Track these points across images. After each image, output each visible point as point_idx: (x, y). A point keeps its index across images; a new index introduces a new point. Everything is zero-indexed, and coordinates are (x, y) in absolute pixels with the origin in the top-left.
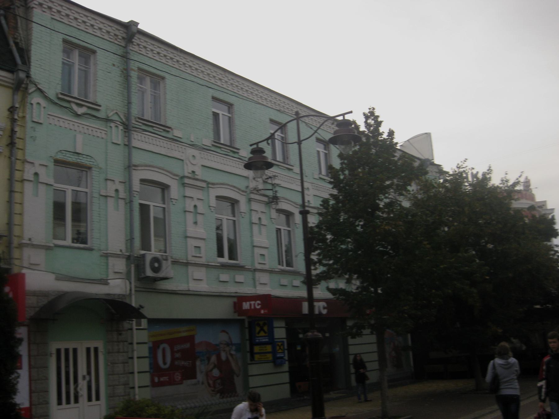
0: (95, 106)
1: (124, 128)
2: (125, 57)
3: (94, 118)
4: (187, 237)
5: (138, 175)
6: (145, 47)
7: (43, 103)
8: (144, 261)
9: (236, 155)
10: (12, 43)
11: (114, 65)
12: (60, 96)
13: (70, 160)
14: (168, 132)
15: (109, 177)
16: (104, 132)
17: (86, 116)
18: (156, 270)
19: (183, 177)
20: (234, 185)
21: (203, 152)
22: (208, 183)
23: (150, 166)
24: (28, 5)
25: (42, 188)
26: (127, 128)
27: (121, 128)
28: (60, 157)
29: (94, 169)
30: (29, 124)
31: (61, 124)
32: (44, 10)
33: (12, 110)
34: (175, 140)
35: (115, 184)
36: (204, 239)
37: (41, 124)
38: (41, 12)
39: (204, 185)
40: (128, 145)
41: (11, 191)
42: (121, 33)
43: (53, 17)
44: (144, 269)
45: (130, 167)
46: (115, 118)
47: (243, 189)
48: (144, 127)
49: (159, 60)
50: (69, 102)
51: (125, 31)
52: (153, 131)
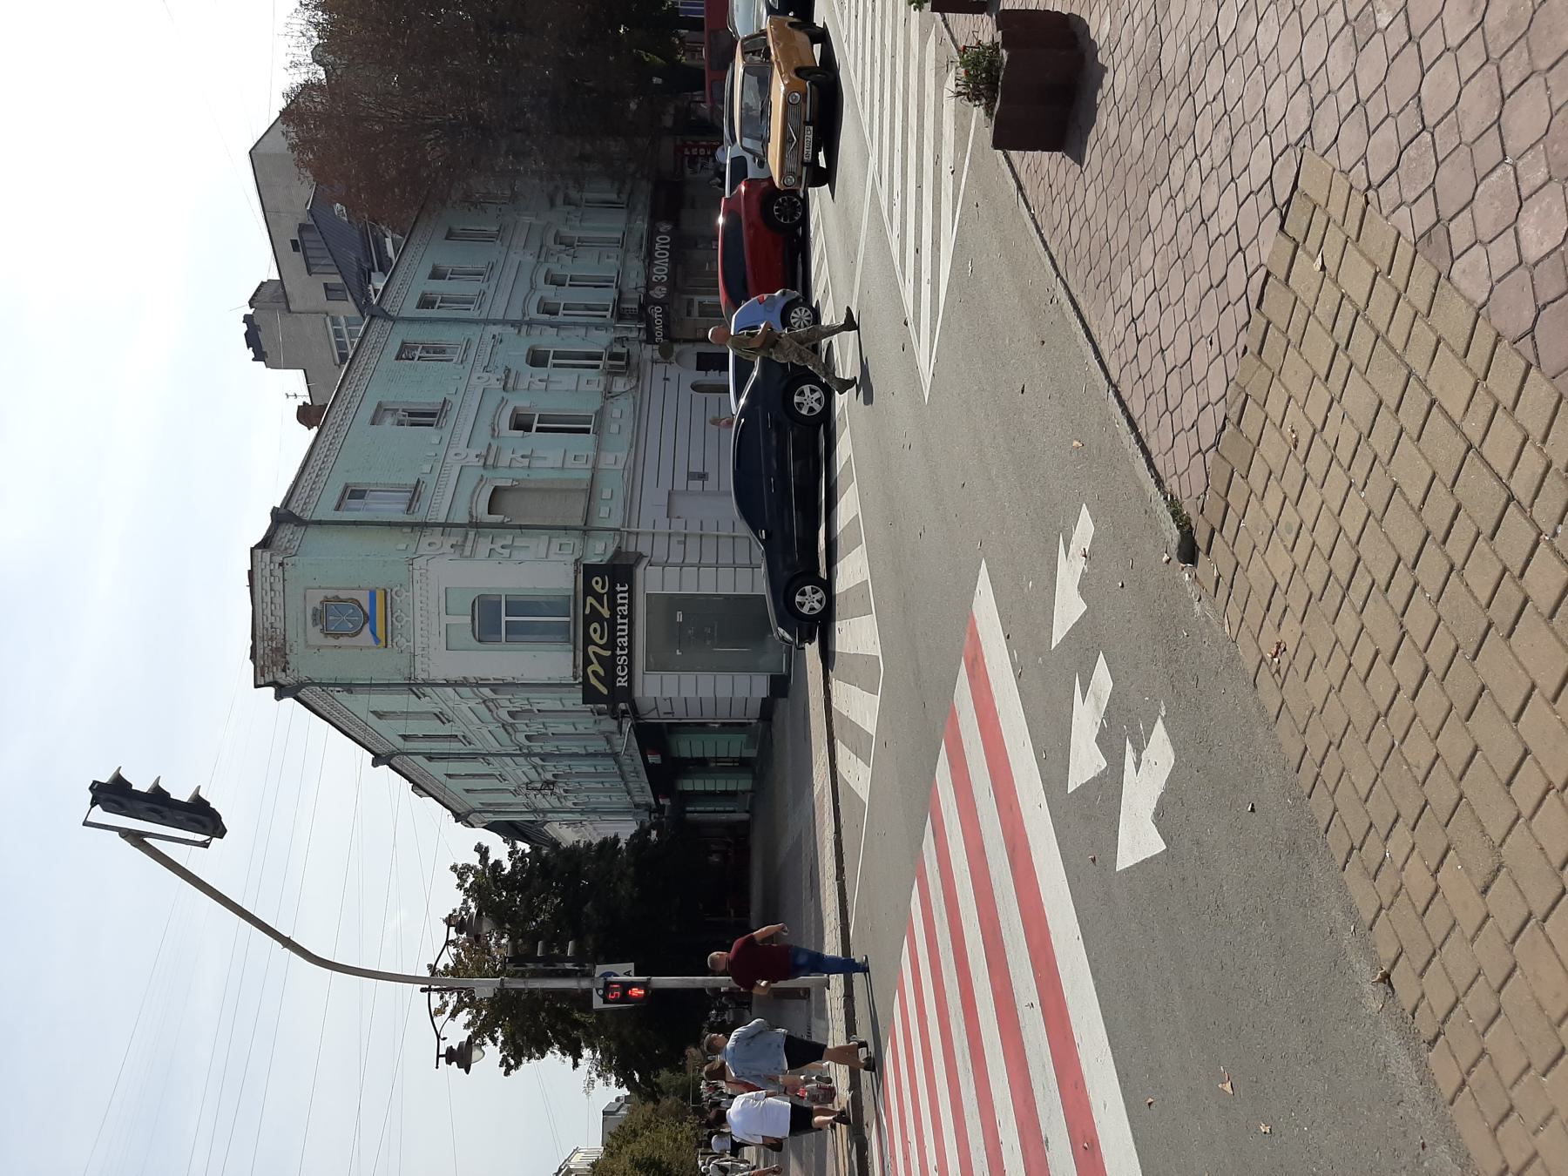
4: (563, 468)
35: (494, 549)
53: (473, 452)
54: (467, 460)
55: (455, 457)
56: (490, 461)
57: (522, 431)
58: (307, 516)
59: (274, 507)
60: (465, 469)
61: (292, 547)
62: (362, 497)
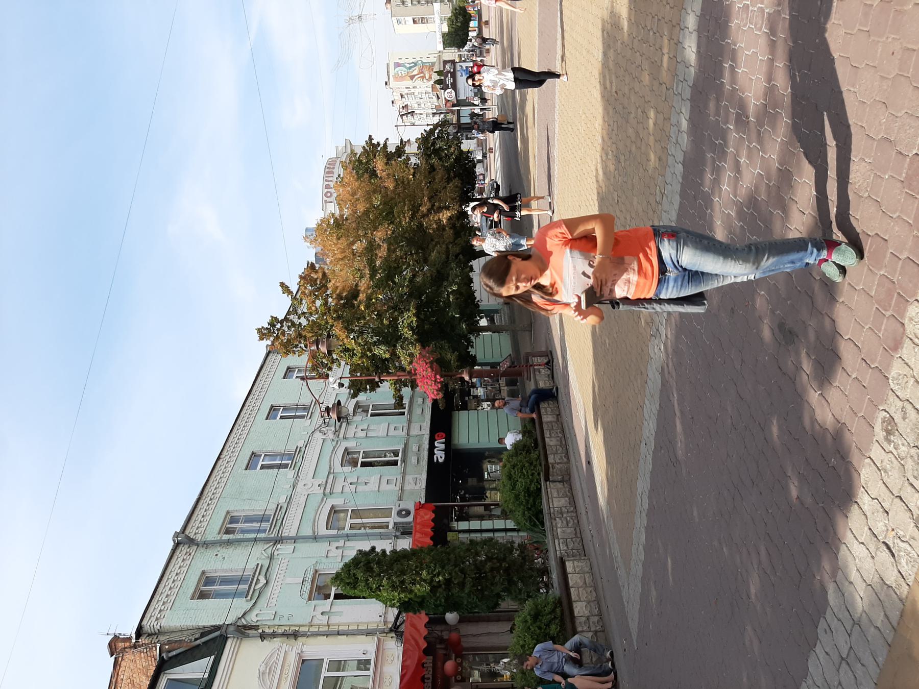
0: (258, 568)
1: (279, 543)
2: (207, 545)
3: (270, 569)
5: (322, 530)
6: (198, 528)
8: (400, 523)
9: (303, 449)
10: (198, 642)
11: (217, 555)
12: (249, 598)
13: (309, 588)
14: (281, 507)
15: (324, 554)
16: (283, 561)
17: (268, 576)
18: (408, 513)
19: (324, 494)
20: (331, 451)
21: (301, 478)
22: (329, 473)
23: (314, 521)
24: (157, 632)
25: (334, 609)
26: (279, 540)
27: (279, 546)
28: (306, 596)
29: (317, 568)
30: (276, 622)
31: (276, 596)
32: (162, 617)
33: (263, 637)
34: (289, 501)
36: (381, 476)
39: (331, 476)
40: (295, 539)
41: (339, 633)
42: (184, 549)
43: (169, 608)
44: (406, 523)
45: (315, 538)
46: (269, 551)
47: (334, 443)
48: (277, 528)
49: (210, 516)
50: (254, 590)
51: (182, 545)
52: (281, 520)
55: (306, 487)
56: (328, 491)
58: (199, 538)
59: (176, 532)
61: (185, 565)
62: (237, 522)
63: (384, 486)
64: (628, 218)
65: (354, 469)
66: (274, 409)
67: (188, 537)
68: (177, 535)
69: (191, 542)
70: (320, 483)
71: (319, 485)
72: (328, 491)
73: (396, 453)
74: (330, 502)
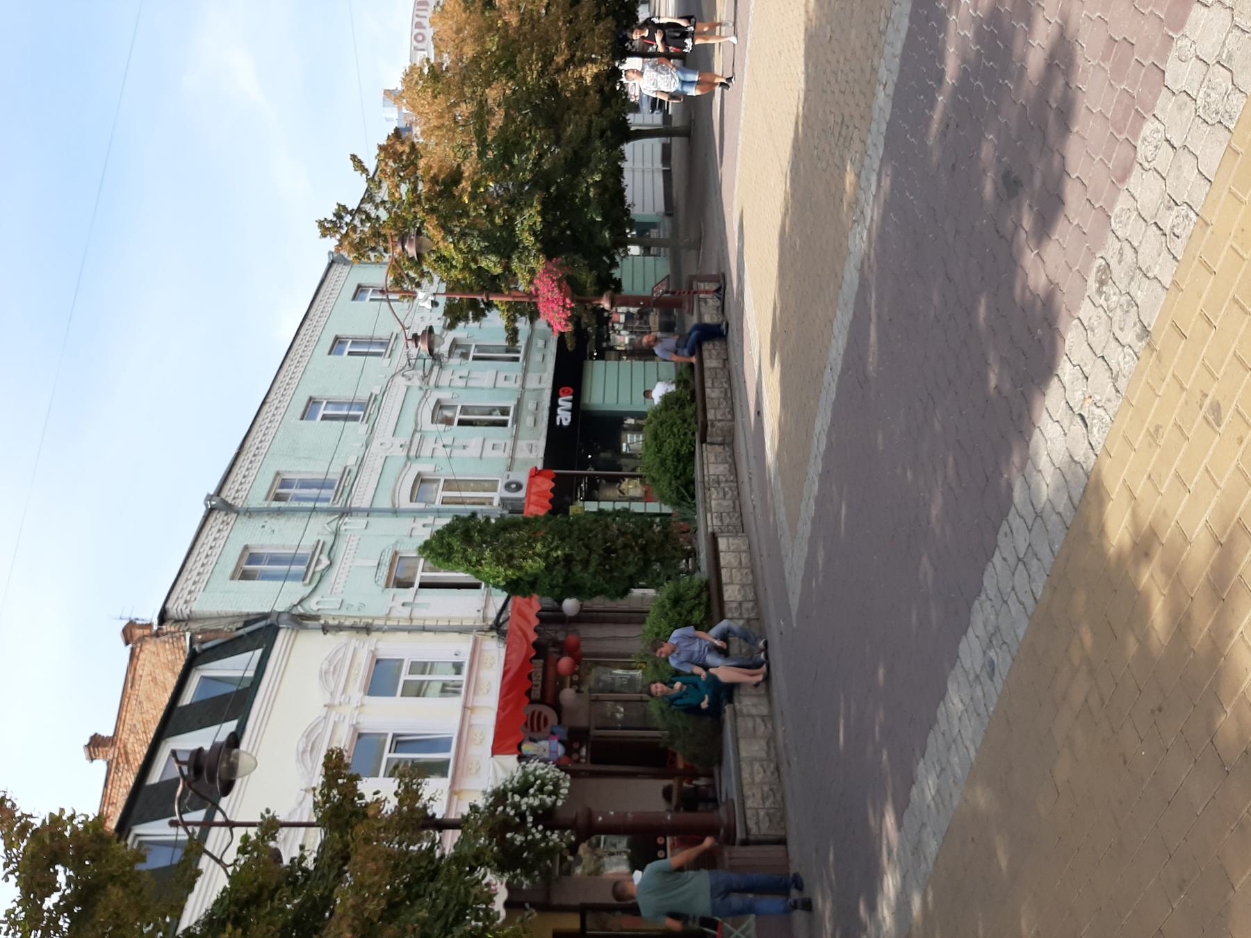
0: (318, 547)
1: (347, 516)
2: (250, 513)
3: (335, 548)
5: (404, 502)
6: (238, 491)
7: (315, 599)
8: (508, 499)
9: (379, 398)
10: (241, 632)
11: (263, 527)
12: (307, 581)
13: (386, 573)
14: (350, 471)
15: (407, 532)
16: (352, 538)
17: (332, 557)
18: (519, 487)
19: (408, 457)
20: (417, 403)
21: (377, 434)
22: (415, 431)
23: (394, 491)
24: (186, 616)
25: (419, 599)
26: (346, 512)
27: (347, 520)
28: (382, 582)
29: (397, 549)
30: (343, 612)
31: (342, 581)
32: (193, 599)
33: (325, 629)
34: (361, 463)
36: (484, 440)
37: (342, 601)
38: (196, 602)
39: (418, 435)
40: (369, 512)
41: (424, 629)
42: (218, 517)
44: (517, 499)
45: (395, 512)
46: (334, 525)
47: (421, 393)
48: (345, 496)
49: (253, 477)
50: (314, 573)
51: (216, 512)
52: (350, 486)
53: (399, 441)
54: (391, 450)
55: (383, 447)
56: (413, 453)
57: (444, 425)
58: (239, 503)
60: (388, 460)
62: (290, 487)
63: (488, 452)
64: (842, 60)
65: (448, 428)
66: (338, 343)
67: (224, 502)
68: (209, 498)
69: (228, 508)
70: (403, 443)
71: (401, 446)
72: (413, 453)
73: (504, 411)
74: (435, 395)
